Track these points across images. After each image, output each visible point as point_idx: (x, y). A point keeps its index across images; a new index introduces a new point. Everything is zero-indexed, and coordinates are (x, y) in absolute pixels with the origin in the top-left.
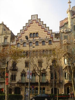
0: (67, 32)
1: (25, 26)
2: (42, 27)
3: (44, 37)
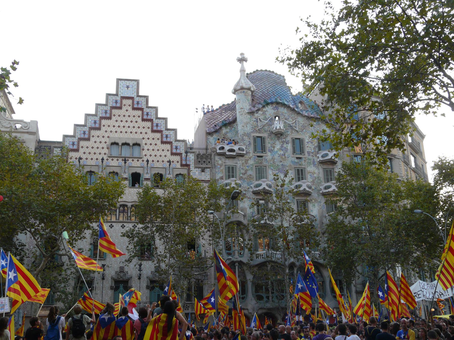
0: (234, 154)
1: (93, 112)
2: (152, 126)
3: (160, 159)
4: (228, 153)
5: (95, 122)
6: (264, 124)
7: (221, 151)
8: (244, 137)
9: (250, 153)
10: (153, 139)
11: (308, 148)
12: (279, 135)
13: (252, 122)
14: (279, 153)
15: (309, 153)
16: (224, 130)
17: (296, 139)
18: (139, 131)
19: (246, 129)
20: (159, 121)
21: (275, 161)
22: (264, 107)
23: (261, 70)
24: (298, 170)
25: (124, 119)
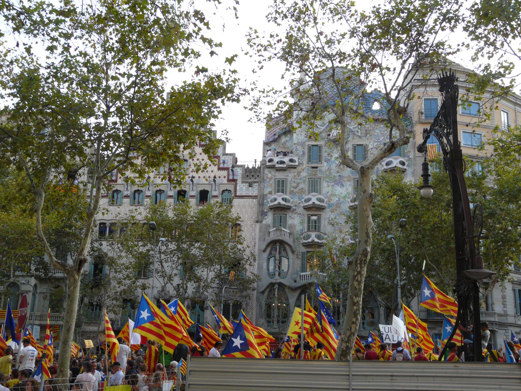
0: (285, 166)
4: (277, 166)
6: (321, 130)
7: (270, 164)
8: (298, 147)
9: (303, 164)
17: (358, 145)
19: (300, 138)
21: (332, 171)
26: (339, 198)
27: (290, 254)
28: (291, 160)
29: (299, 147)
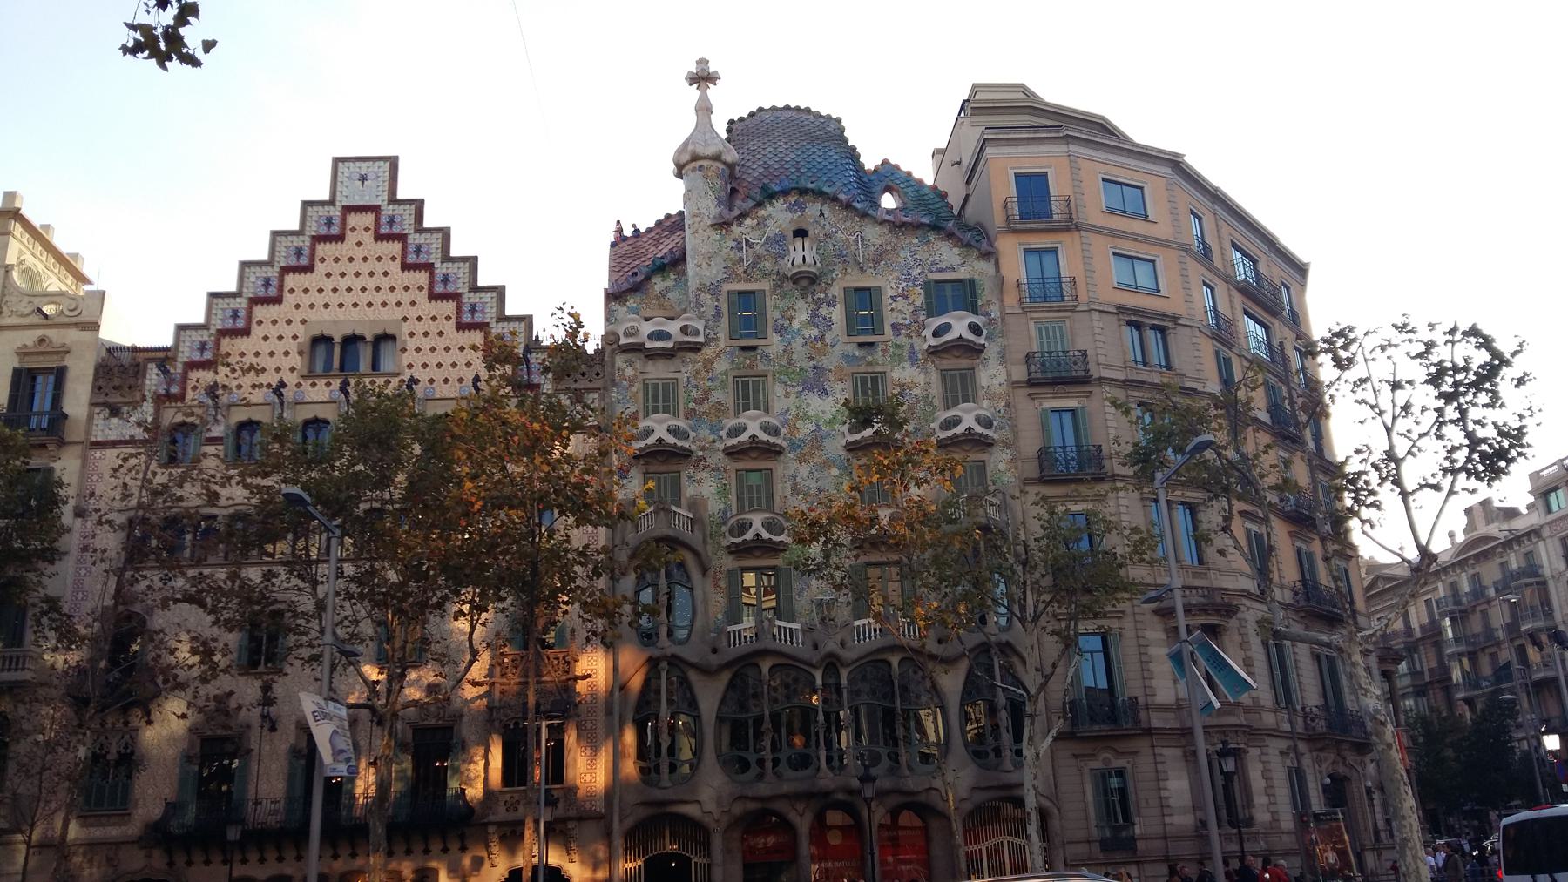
0: (670, 345)
2: (431, 283)
3: (453, 375)
4: (649, 345)
5: (267, 283)
7: (631, 340)
9: (718, 339)
10: (434, 318)
11: (895, 314)
12: (807, 282)
13: (725, 251)
14: (806, 333)
15: (896, 328)
16: (658, 284)
17: (857, 290)
18: (392, 298)
20: (451, 268)
21: (795, 356)
22: (760, 205)
23: (774, 109)
24: (864, 381)
25: (350, 269)
26: (817, 425)
27: (696, 575)
28: (684, 330)
29: (706, 298)
